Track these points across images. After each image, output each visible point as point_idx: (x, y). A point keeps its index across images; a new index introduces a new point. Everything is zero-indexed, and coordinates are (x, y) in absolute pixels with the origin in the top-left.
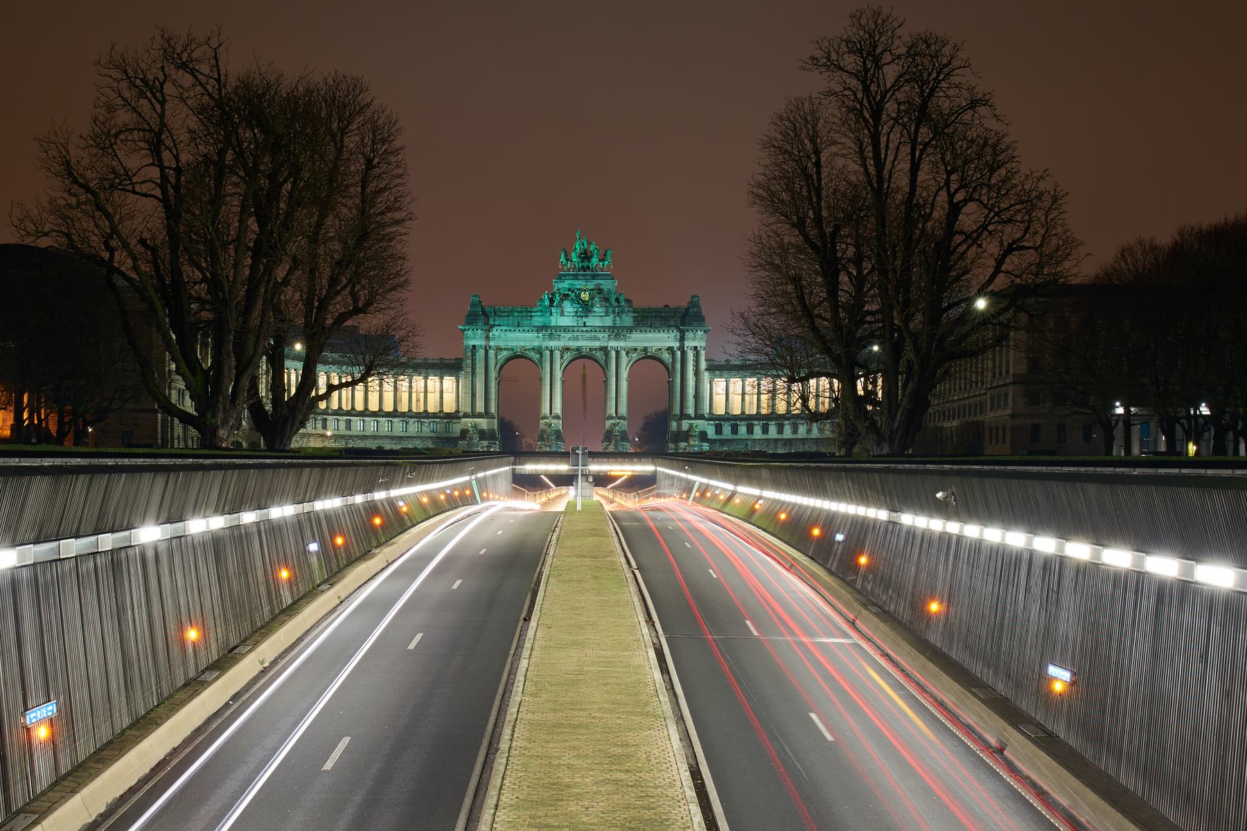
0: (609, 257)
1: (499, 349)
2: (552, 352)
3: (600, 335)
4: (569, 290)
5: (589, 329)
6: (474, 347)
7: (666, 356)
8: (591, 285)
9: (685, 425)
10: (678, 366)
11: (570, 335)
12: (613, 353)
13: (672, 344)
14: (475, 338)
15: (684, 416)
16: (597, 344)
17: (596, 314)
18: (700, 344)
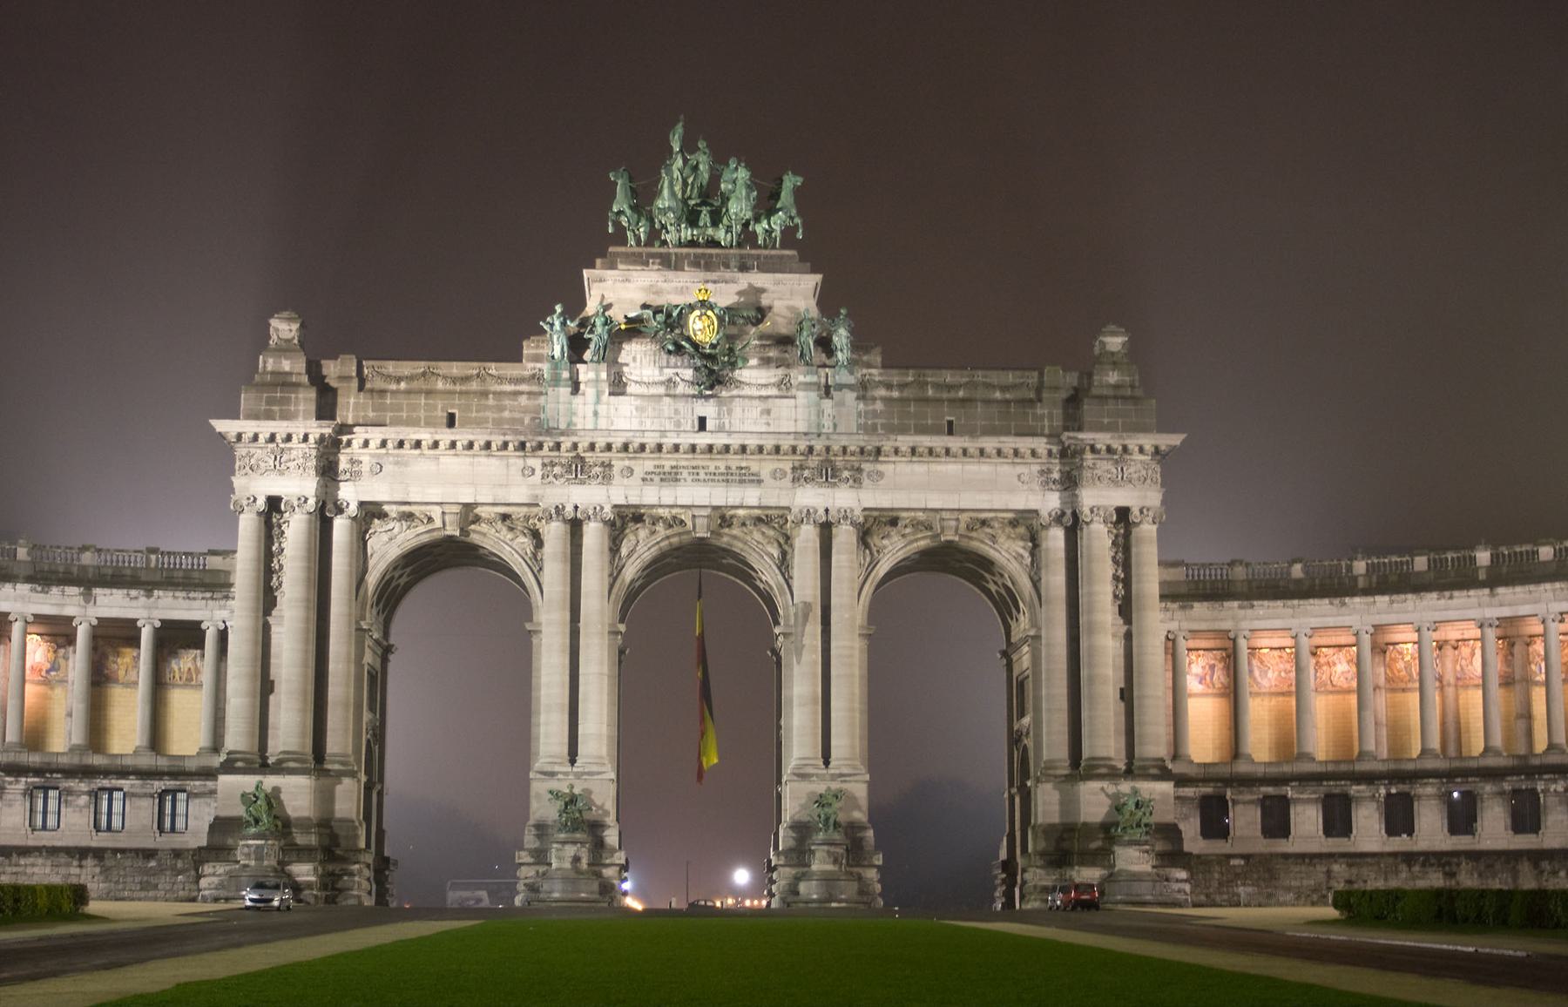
0: (786, 197)
1: (371, 512)
2: (575, 527)
3: (765, 467)
4: (645, 306)
5: (720, 440)
6: (274, 503)
7: (1008, 553)
8: (726, 293)
9: (1094, 800)
10: (1056, 580)
11: (649, 465)
12: (806, 538)
13: (1021, 501)
14: (279, 468)
15: (1080, 767)
16: (751, 496)
17: (747, 391)
18: (1143, 497)
